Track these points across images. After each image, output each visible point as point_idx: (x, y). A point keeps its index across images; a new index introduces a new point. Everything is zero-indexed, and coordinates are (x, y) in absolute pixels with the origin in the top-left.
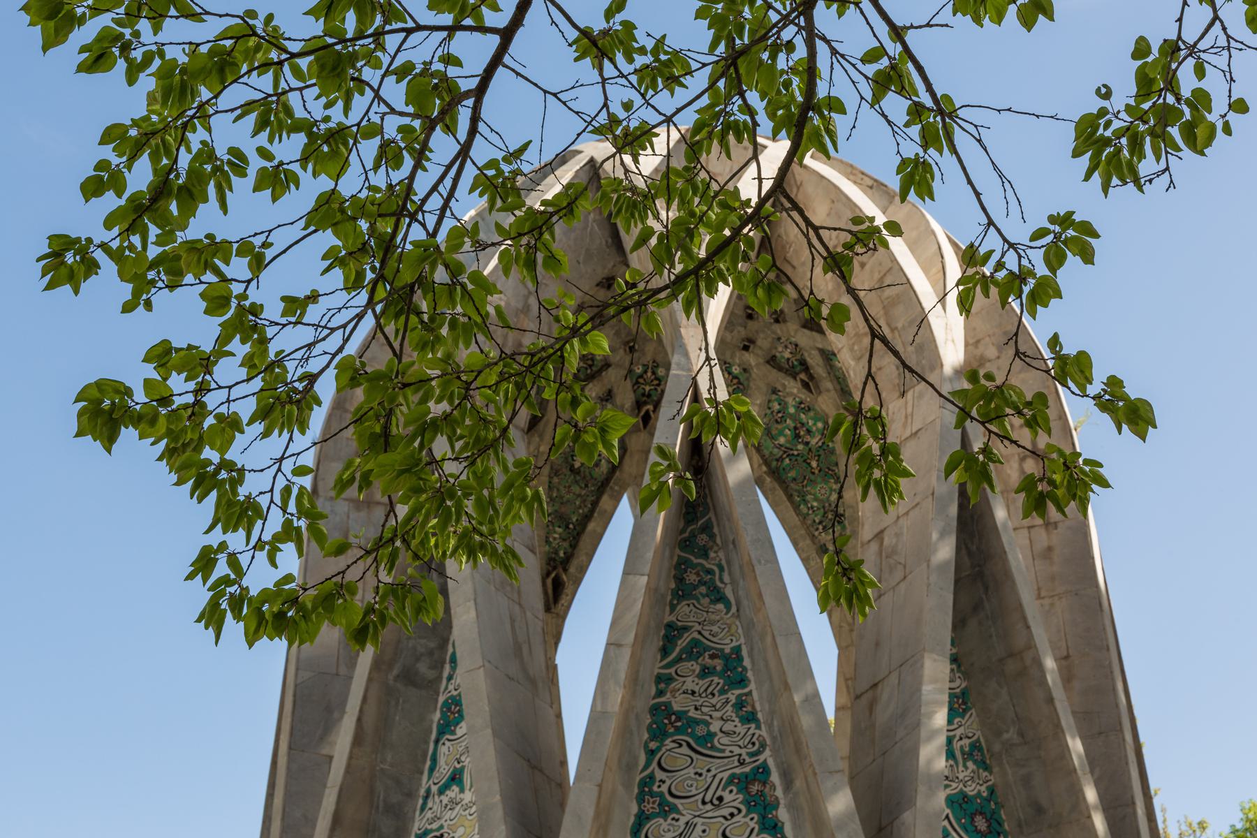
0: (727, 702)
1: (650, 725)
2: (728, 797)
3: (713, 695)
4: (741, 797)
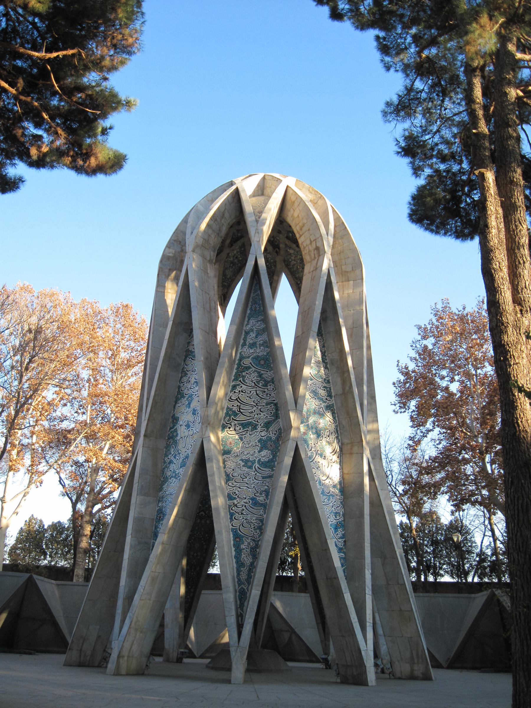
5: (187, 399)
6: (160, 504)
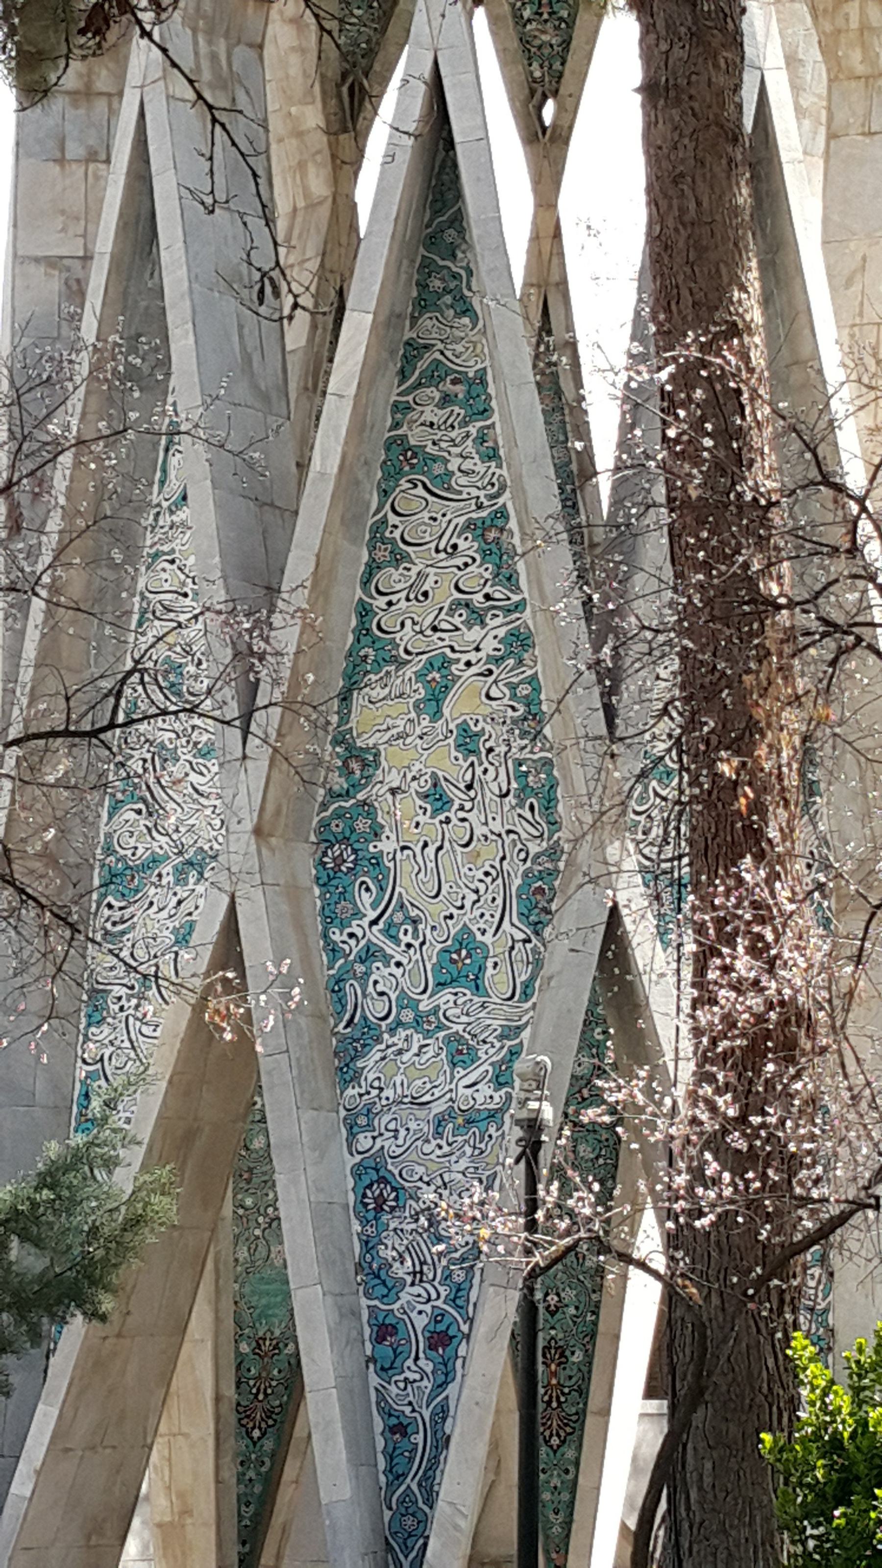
0: (468, 436)
1: (384, 462)
2: (462, 545)
3: (453, 427)
4: (476, 545)
5: (420, 676)
6: (364, 1141)
